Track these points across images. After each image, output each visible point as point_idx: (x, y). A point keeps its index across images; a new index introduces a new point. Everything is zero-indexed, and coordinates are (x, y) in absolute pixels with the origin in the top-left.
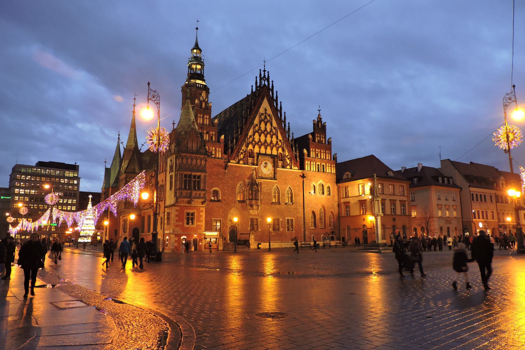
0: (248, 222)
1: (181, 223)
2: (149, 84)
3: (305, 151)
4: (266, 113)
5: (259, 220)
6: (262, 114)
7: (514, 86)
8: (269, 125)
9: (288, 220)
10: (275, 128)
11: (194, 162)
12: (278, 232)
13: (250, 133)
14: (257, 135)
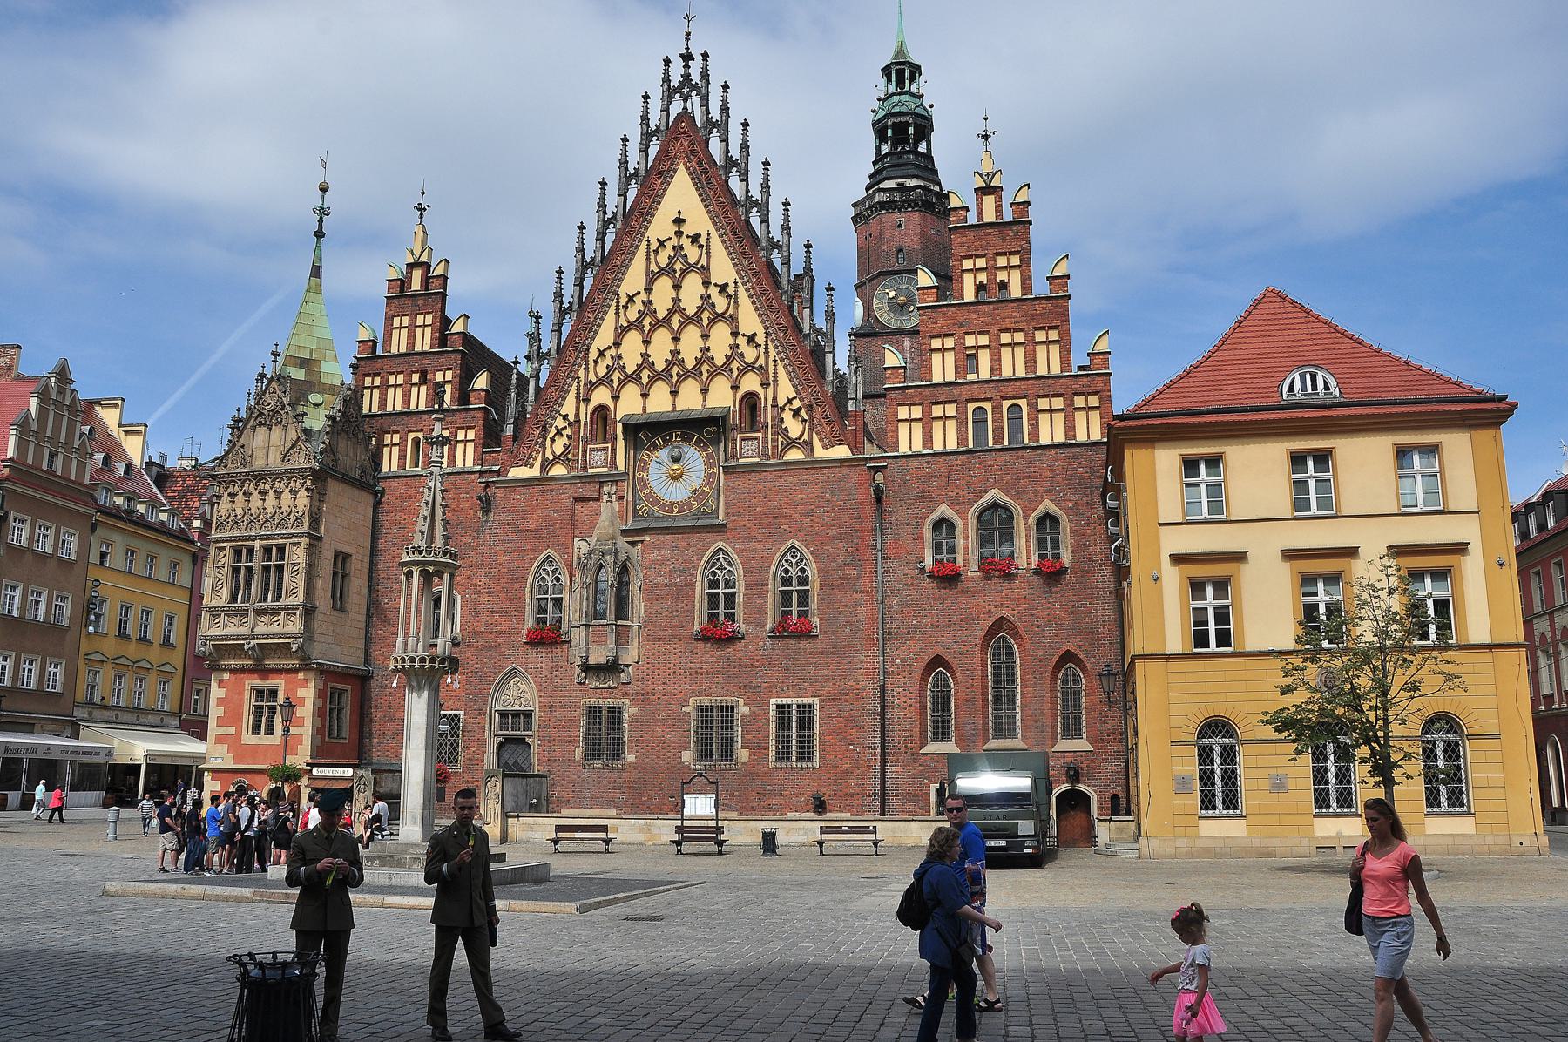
1: (232, 730)
6: (661, 244)
8: (693, 284)
9: (784, 710)
10: (723, 288)
11: (271, 499)
12: (726, 764)
13: (604, 337)
14: (633, 341)
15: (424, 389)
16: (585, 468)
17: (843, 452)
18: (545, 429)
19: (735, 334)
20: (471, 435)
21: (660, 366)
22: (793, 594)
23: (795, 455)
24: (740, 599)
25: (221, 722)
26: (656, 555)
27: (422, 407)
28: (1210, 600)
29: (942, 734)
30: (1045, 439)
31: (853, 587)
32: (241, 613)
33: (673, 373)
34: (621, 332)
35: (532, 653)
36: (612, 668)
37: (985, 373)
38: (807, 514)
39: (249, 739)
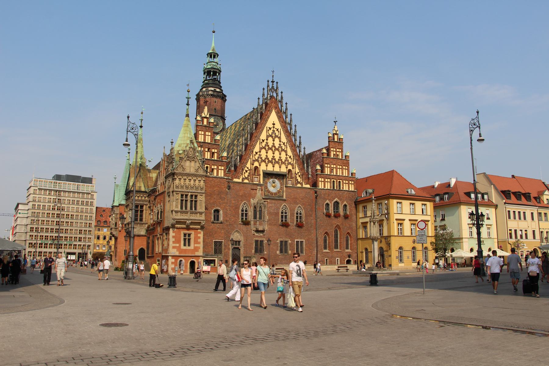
0: (252, 244)
1: (178, 245)
2: (128, 117)
3: (318, 167)
4: (274, 127)
5: (265, 242)
6: (270, 129)
7: (478, 112)
8: (277, 140)
10: (284, 144)
13: (257, 149)
14: (263, 151)
15: (209, 153)
16: (253, 181)
17: (308, 186)
18: (243, 170)
19: (286, 155)
20: (223, 168)
21: (270, 159)
22: (299, 216)
23: (299, 185)
24: (288, 217)
25: (174, 242)
26: (270, 205)
27: (209, 158)
28: (399, 227)
29: (325, 248)
30: (345, 189)
31: (311, 216)
32: (187, 213)
33: (273, 161)
34: (261, 149)
35: (242, 226)
36: (263, 231)
37: (335, 174)
38: (302, 199)
39: (183, 247)
